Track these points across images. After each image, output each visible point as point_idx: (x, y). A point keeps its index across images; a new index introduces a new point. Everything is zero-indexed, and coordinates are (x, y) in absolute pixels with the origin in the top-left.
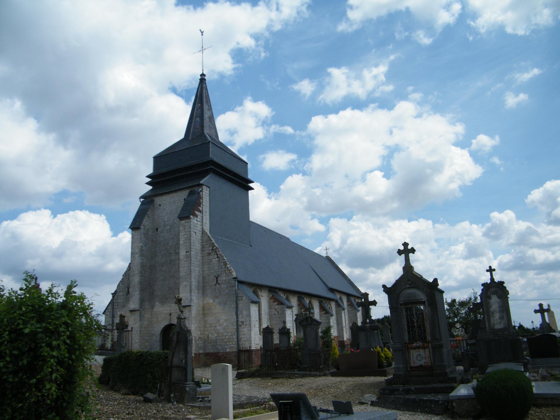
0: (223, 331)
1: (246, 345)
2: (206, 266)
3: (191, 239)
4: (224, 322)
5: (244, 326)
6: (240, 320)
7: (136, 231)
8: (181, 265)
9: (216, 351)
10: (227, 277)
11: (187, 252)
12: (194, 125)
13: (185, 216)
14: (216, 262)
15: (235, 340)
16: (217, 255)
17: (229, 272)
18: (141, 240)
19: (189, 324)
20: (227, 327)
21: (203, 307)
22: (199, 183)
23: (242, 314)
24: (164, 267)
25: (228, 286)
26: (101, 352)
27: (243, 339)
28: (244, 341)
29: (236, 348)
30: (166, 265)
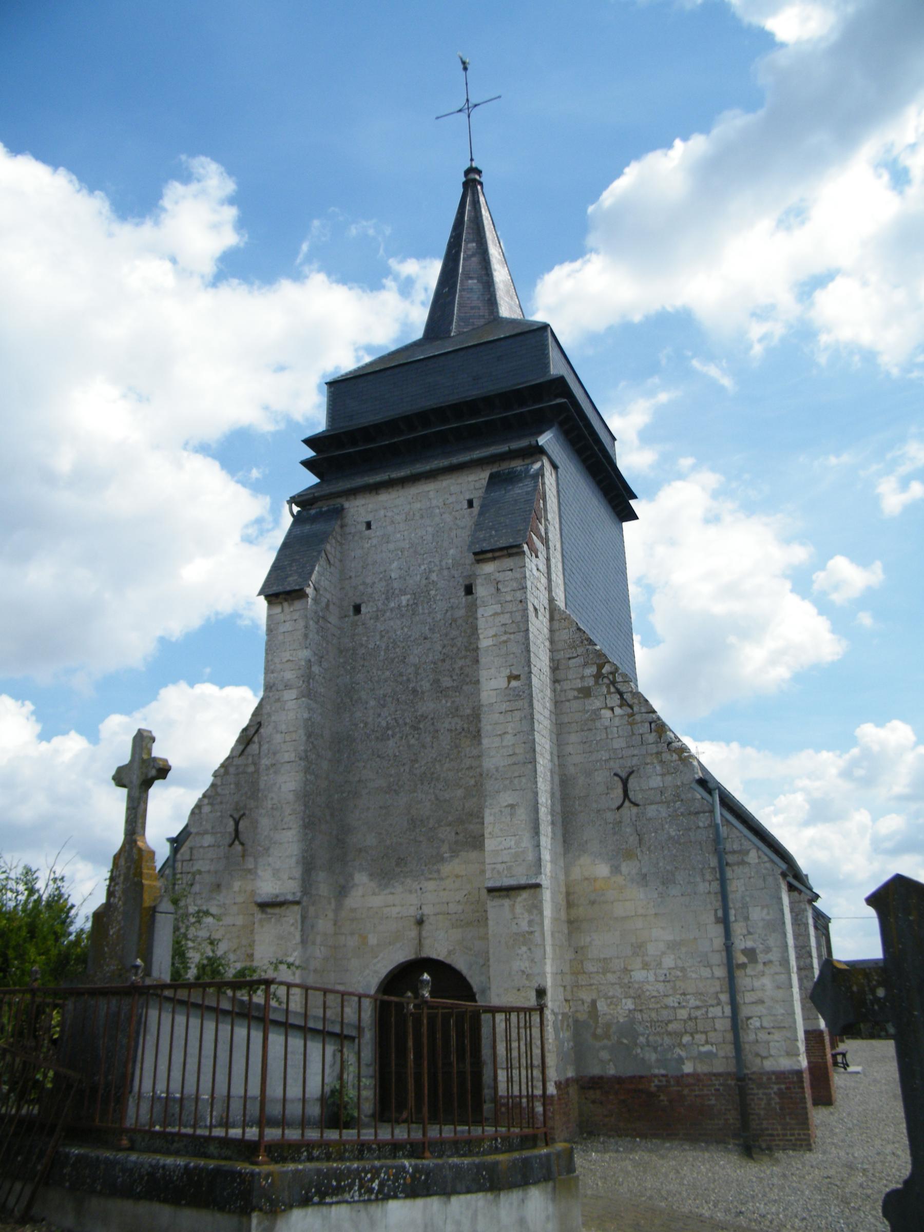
0: (661, 987)
1: (772, 1044)
2: (573, 738)
3: (527, 630)
4: (664, 953)
5: (760, 967)
6: (740, 943)
7: (286, 605)
8: (489, 727)
9: (628, 1070)
10: (669, 778)
11: (512, 677)
12: (460, 297)
13: (502, 543)
14: (617, 721)
15: (717, 1026)
16: (621, 694)
17: (675, 757)
18: (306, 636)
19: (532, 961)
20: (679, 973)
21: (568, 894)
22: (533, 442)
23: (747, 919)
24: (391, 743)
25: (675, 811)
26: (416, 1169)
27: (755, 1023)
28: (762, 1027)
29: (727, 1058)
30: (398, 735)
